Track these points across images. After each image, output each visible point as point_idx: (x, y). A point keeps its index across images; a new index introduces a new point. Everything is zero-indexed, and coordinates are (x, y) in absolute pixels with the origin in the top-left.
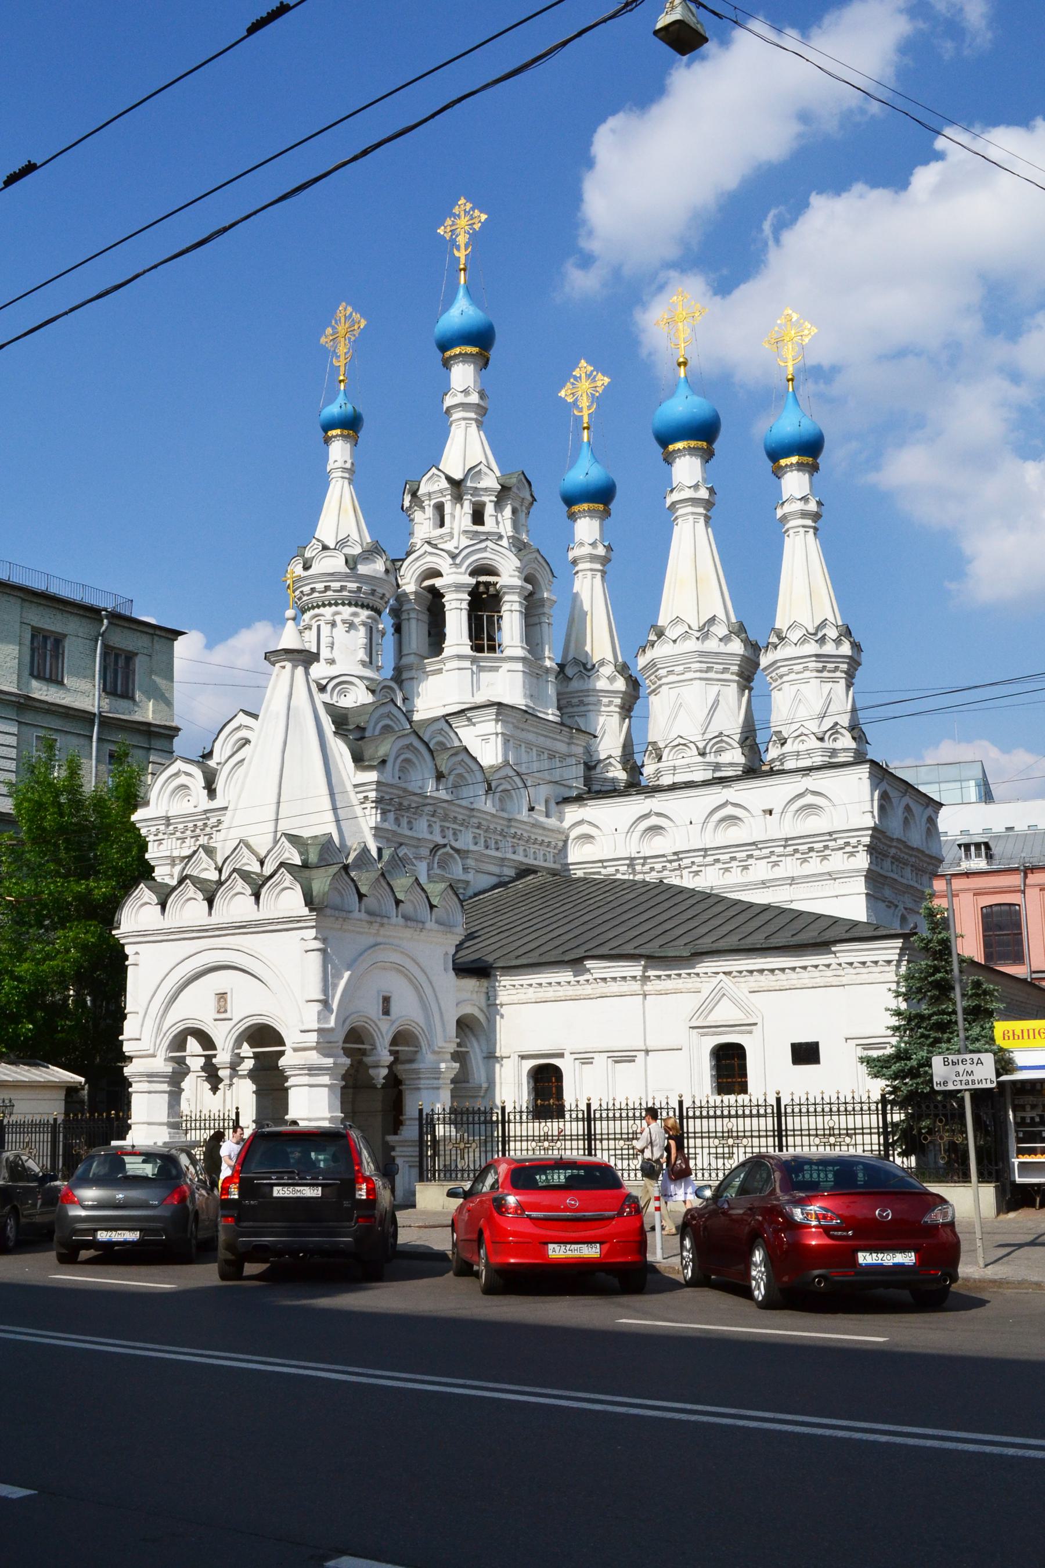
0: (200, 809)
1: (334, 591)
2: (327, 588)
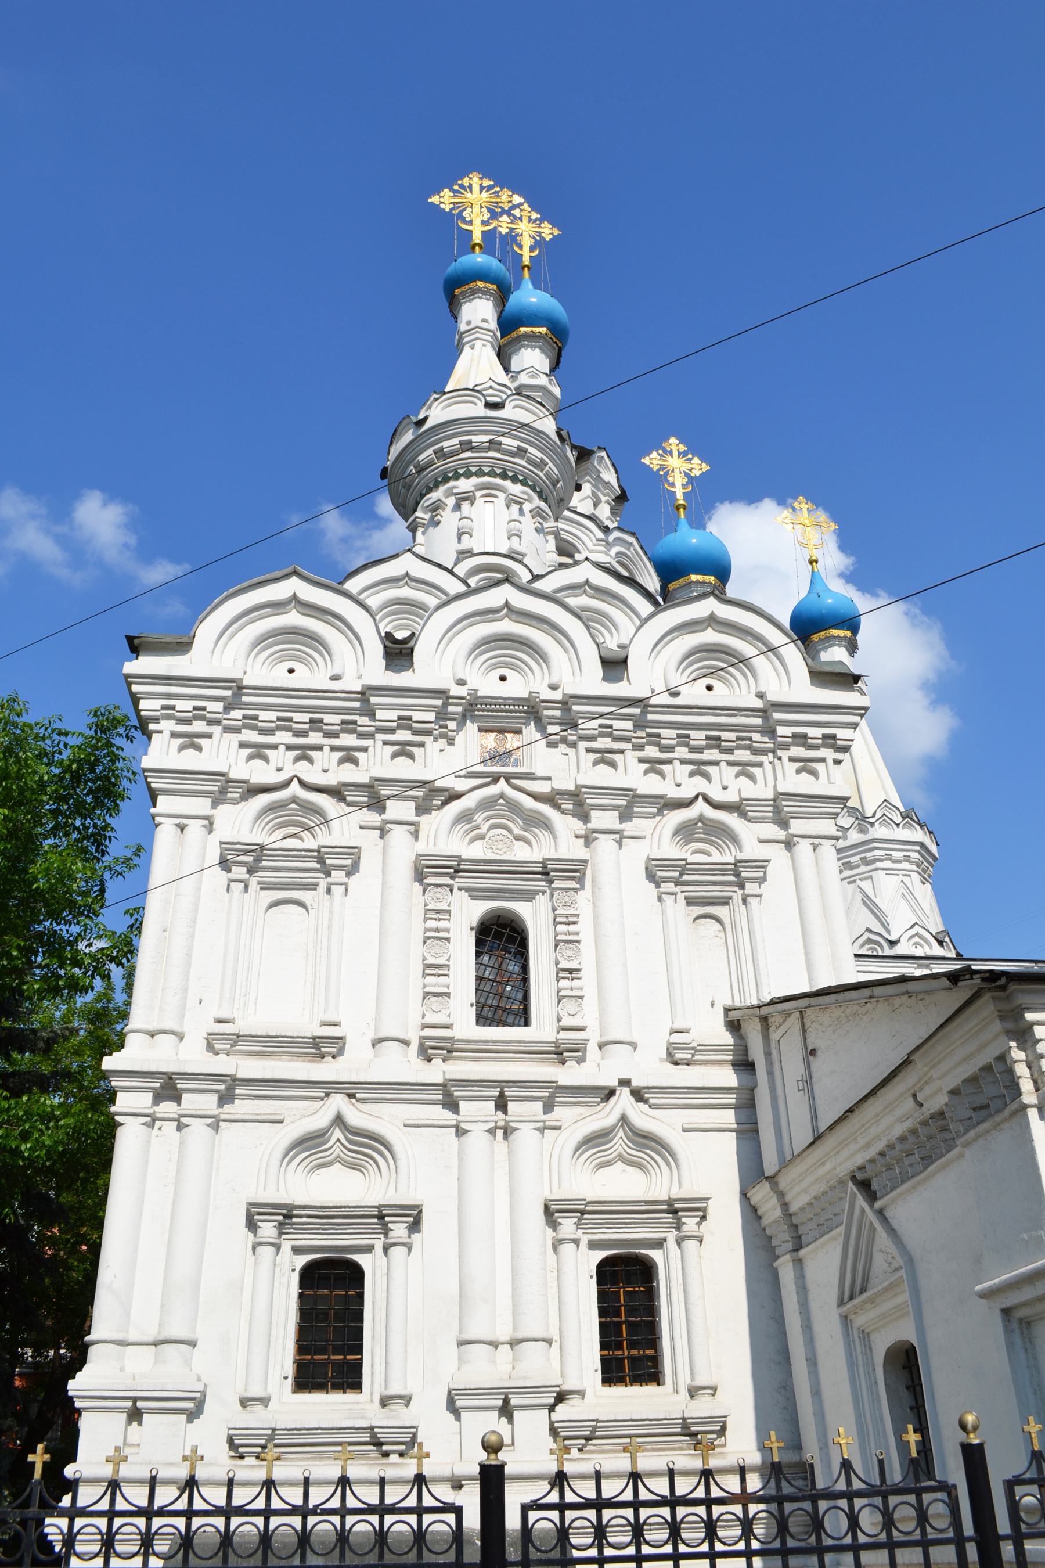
0: (352, 683)
1: (530, 461)
2: (521, 452)
